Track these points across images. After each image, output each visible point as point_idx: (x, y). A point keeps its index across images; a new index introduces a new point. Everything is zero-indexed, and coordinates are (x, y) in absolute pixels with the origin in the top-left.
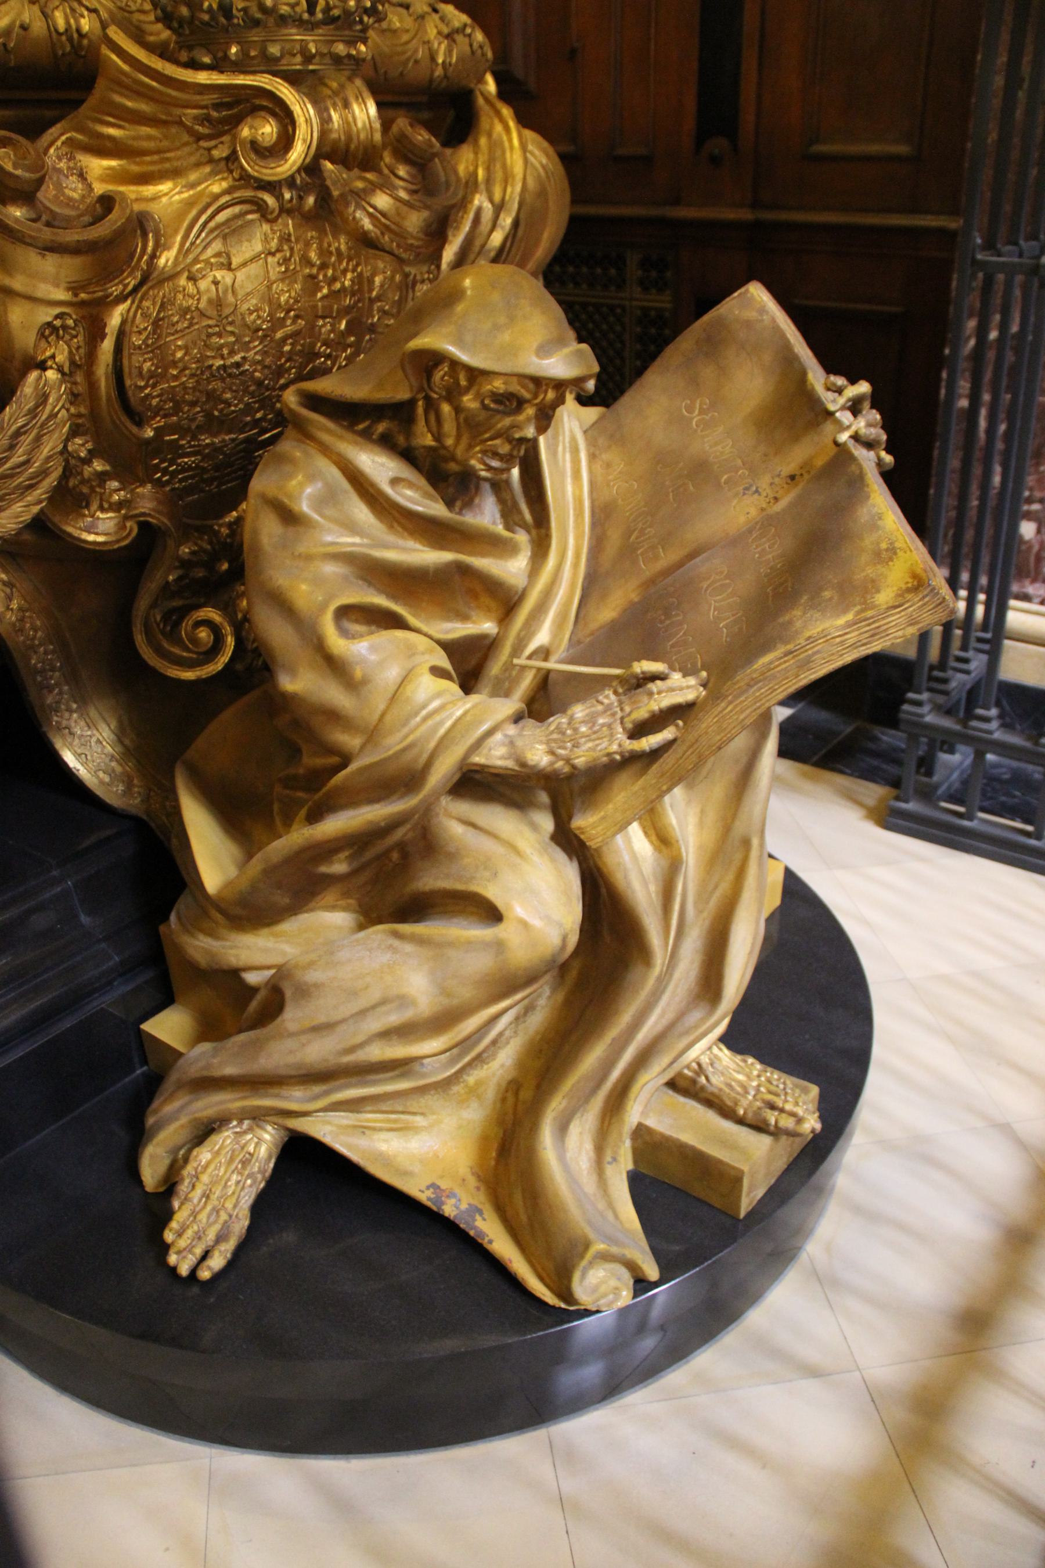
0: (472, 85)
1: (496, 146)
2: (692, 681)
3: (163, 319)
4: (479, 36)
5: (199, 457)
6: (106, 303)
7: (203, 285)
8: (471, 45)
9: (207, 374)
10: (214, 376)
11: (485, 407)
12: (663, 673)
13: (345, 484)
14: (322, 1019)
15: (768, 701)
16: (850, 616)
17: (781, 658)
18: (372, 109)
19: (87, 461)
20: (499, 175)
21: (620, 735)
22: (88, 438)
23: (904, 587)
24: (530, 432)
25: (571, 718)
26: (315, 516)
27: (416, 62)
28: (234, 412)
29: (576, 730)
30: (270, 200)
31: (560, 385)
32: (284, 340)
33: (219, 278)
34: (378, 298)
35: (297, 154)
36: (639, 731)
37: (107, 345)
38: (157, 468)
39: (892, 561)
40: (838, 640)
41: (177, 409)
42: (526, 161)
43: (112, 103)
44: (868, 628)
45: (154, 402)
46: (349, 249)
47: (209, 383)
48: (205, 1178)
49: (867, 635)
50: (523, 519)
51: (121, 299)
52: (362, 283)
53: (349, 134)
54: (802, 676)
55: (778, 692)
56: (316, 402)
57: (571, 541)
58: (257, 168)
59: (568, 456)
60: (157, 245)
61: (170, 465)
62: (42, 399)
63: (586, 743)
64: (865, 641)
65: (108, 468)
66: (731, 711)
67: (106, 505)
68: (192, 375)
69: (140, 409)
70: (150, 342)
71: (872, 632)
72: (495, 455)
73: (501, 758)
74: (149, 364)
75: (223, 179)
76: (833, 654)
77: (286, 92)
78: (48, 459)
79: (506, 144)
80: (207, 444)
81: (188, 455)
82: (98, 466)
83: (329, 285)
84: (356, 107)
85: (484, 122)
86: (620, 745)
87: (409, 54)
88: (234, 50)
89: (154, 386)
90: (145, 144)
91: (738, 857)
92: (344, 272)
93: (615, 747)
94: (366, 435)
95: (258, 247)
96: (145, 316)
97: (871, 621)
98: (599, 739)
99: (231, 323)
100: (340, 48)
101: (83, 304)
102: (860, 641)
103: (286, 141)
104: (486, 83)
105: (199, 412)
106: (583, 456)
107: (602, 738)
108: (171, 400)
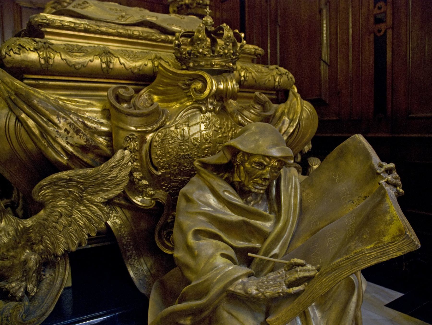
0: (289, 88)
2: (314, 268)
3: (164, 139)
4: (291, 75)
5: (178, 184)
7: (178, 130)
8: (288, 78)
9: (179, 157)
10: (180, 158)
12: (303, 264)
15: (340, 278)
16: (372, 245)
17: (344, 261)
20: (292, 111)
21: (284, 287)
22: (140, 173)
23: (395, 234)
27: (269, 80)
28: (187, 170)
32: (205, 149)
33: (184, 128)
36: (290, 285)
38: (163, 185)
39: (392, 224)
40: (368, 255)
41: (170, 167)
44: (380, 251)
45: (161, 164)
46: (231, 125)
47: (179, 160)
49: (380, 254)
50: (274, 210)
54: (354, 269)
55: (344, 275)
58: (195, 96)
60: (166, 118)
61: (168, 185)
62: (123, 158)
63: (270, 288)
64: (379, 256)
65: (147, 183)
66: (325, 281)
67: (147, 195)
68: (174, 157)
69: (156, 165)
70: (160, 145)
71: (382, 252)
73: (240, 289)
74: (159, 152)
75: (191, 102)
76: (366, 261)
78: (124, 177)
79: (297, 104)
80: (180, 179)
81: (174, 182)
82: (145, 182)
83: (222, 134)
86: (283, 290)
87: (267, 78)
89: (161, 159)
92: (229, 131)
96: (159, 137)
97: (381, 248)
98: (275, 286)
99: (187, 142)
101: (139, 131)
102: (377, 256)
104: (294, 89)
105: (176, 169)
107: (277, 286)
108: (167, 164)
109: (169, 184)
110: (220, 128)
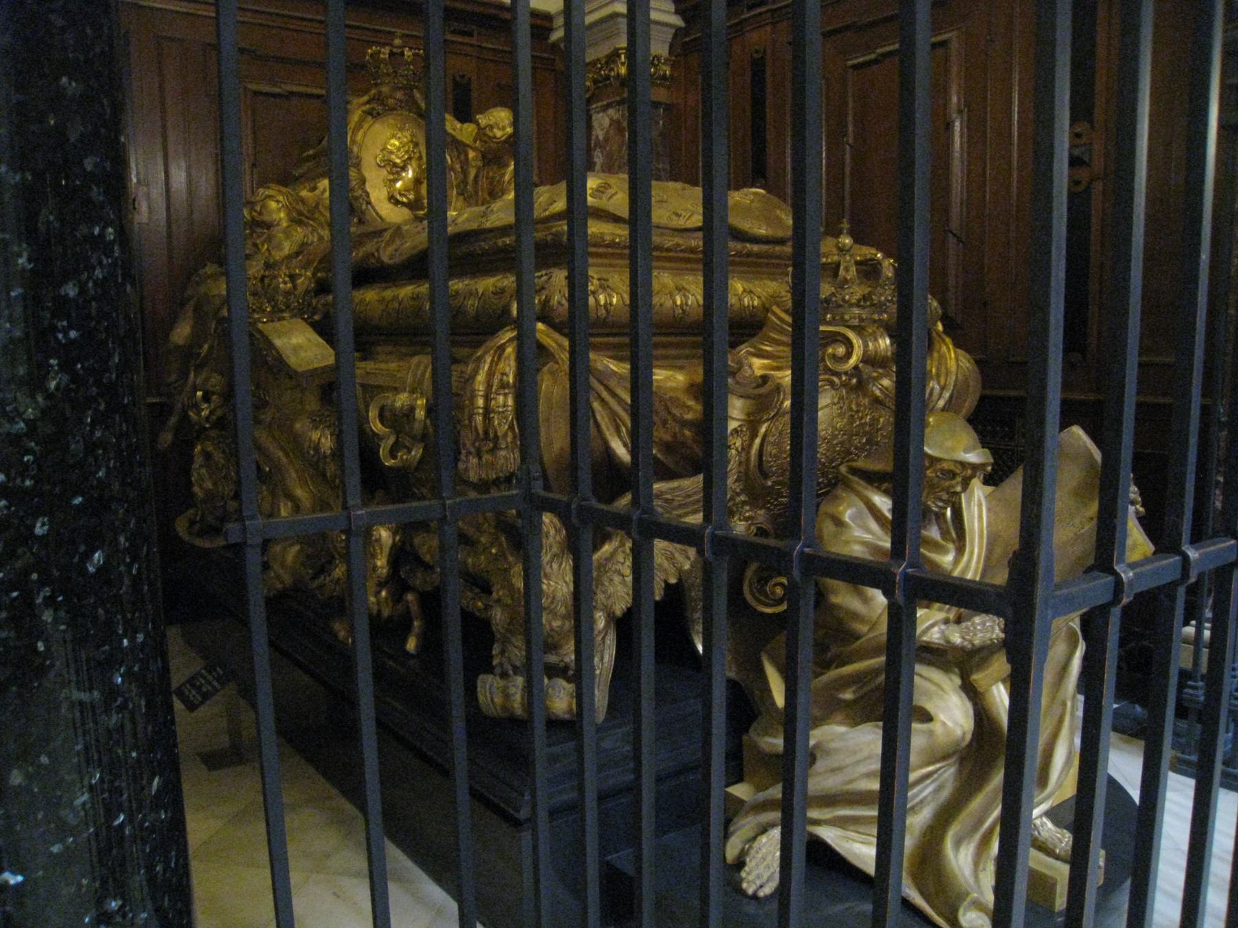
1: (942, 358)
6: (760, 422)
11: (937, 476)
13: (866, 511)
14: (837, 765)
18: (888, 341)
19: (738, 494)
20: (943, 370)
24: (959, 489)
25: (973, 624)
26: (850, 523)
29: (975, 628)
30: (836, 379)
31: (975, 467)
34: (881, 429)
35: (853, 361)
37: (758, 441)
38: (769, 502)
42: (958, 366)
43: (769, 337)
48: (764, 850)
51: (768, 420)
52: (874, 420)
53: (876, 352)
56: (855, 471)
57: (976, 551)
59: (976, 508)
72: (941, 500)
77: (851, 335)
84: (880, 341)
85: (937, 346)
88: (829, 316)
90: (781, 354)
91: (1059, 712)
93: (994, 636)
94: (878, 488)
95: (828, 401)
100: (876, 317)
103: (849, 355)
106: (984, 509)
109: (776, 500)
110: (858, 412)
